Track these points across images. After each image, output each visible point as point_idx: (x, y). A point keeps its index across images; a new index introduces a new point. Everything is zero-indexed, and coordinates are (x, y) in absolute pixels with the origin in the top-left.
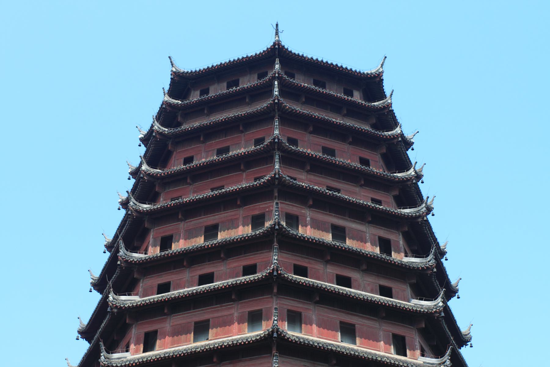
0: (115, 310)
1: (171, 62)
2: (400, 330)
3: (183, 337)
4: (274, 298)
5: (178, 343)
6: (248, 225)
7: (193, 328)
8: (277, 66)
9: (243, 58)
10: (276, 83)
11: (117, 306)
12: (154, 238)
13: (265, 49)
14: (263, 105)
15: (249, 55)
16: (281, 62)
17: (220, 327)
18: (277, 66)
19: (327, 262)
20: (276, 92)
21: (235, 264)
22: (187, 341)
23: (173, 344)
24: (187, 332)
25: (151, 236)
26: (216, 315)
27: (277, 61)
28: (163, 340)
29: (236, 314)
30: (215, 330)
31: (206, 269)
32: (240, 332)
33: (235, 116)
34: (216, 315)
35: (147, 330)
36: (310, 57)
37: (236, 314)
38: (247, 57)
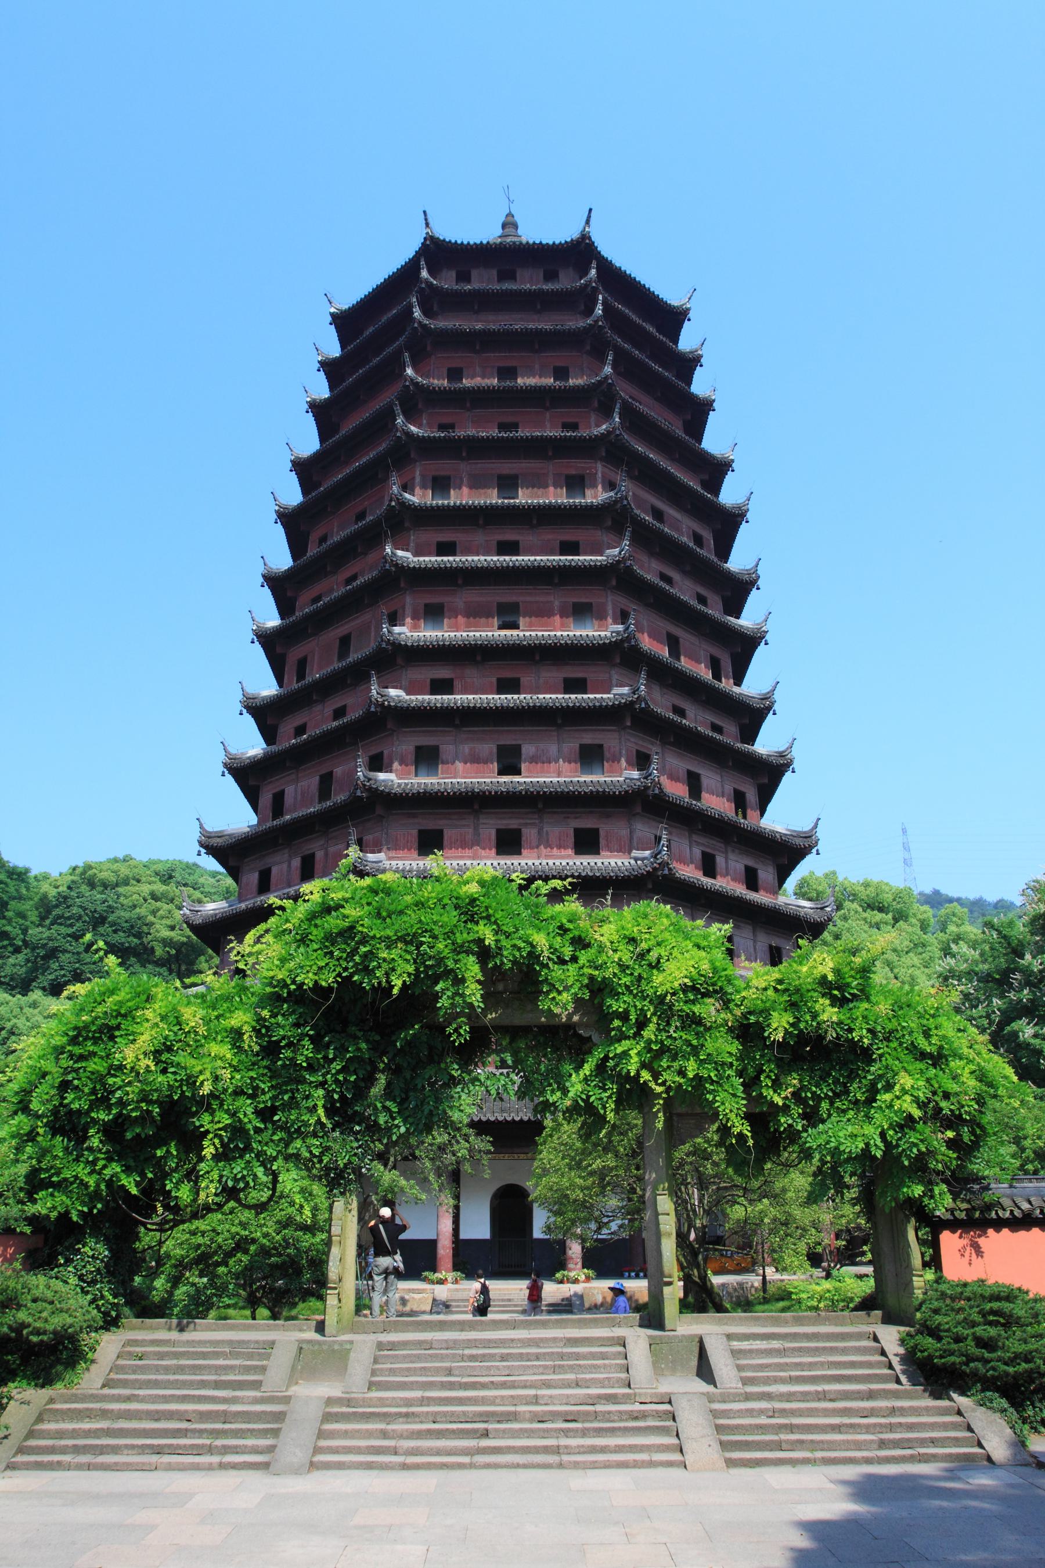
0: (393, 569)
1: (426, 220)
2: (718, 653)
3: (483, 620)
4: (609, 592)
5: (477, 627)
6: (562, 488)
7: (495, 609)
8: (593, 272)
9: (534, 243)
10: (600, 297)
11: (397, 564)
12: (423, 476)
13: (569, 240)
14: (576, 323)
15: (544, 242)
16: (598, 269)
17: (536, 616)
18: (593, 272)
19: (652, 554)
20: (599, 310)
21: (550, 537)
22: (489, 626)
23: (468, 627)
24: (489, 615)
25: (418, 473)
26: (528, 599)
27: (594, 264)
28: (453, 620)
29: (557, 603)
30: (527, 619)
31: (509, 536)
32: (563, 627)
33: (537, 328)
34: (528, 599)
35: (428, 601)
36: (618, 265)
37: (557, 603)
38: (541, 243)
